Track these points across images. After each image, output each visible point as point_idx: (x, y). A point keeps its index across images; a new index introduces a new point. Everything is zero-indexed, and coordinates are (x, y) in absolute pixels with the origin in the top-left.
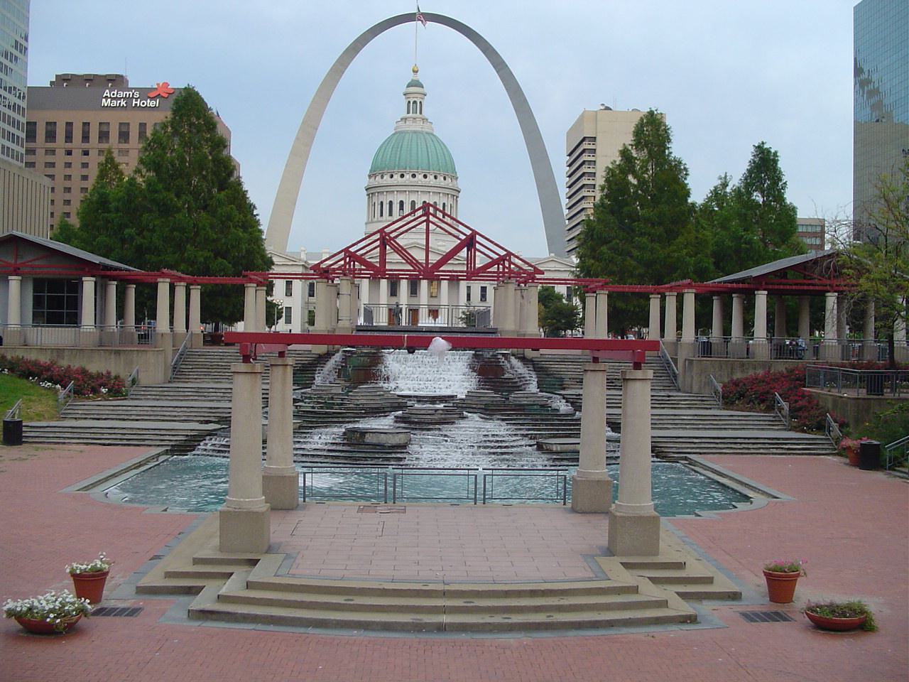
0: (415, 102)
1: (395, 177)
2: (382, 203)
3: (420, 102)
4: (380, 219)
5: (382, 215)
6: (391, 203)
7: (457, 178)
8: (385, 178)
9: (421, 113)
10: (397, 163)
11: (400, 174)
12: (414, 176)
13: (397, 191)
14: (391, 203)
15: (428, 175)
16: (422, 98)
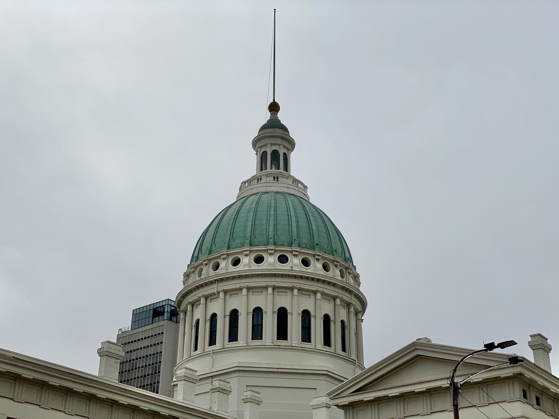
0: (275, 154)
1: (245, 260)
2: (214, 316)
3: (285, 154)
4: (213, 348)
5: (212, 342)
6: (234, 315)
7: (359, 285)
8: (223, 264)
9: (286, 168)
10: (248, 235)
11: (253, 256)
12: (283, 259)
13: (249, 289)
14: (234, 315)
15: (311, 259)
16: (288, 150)
